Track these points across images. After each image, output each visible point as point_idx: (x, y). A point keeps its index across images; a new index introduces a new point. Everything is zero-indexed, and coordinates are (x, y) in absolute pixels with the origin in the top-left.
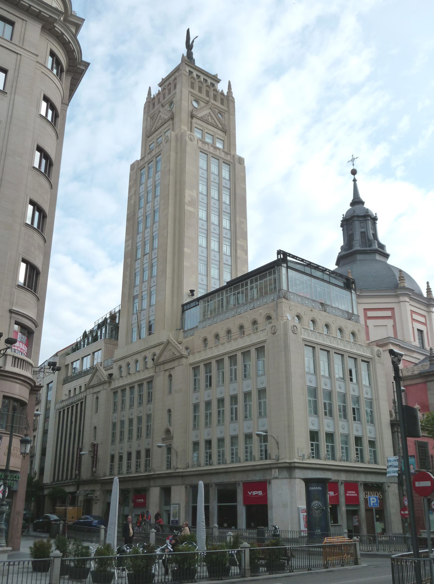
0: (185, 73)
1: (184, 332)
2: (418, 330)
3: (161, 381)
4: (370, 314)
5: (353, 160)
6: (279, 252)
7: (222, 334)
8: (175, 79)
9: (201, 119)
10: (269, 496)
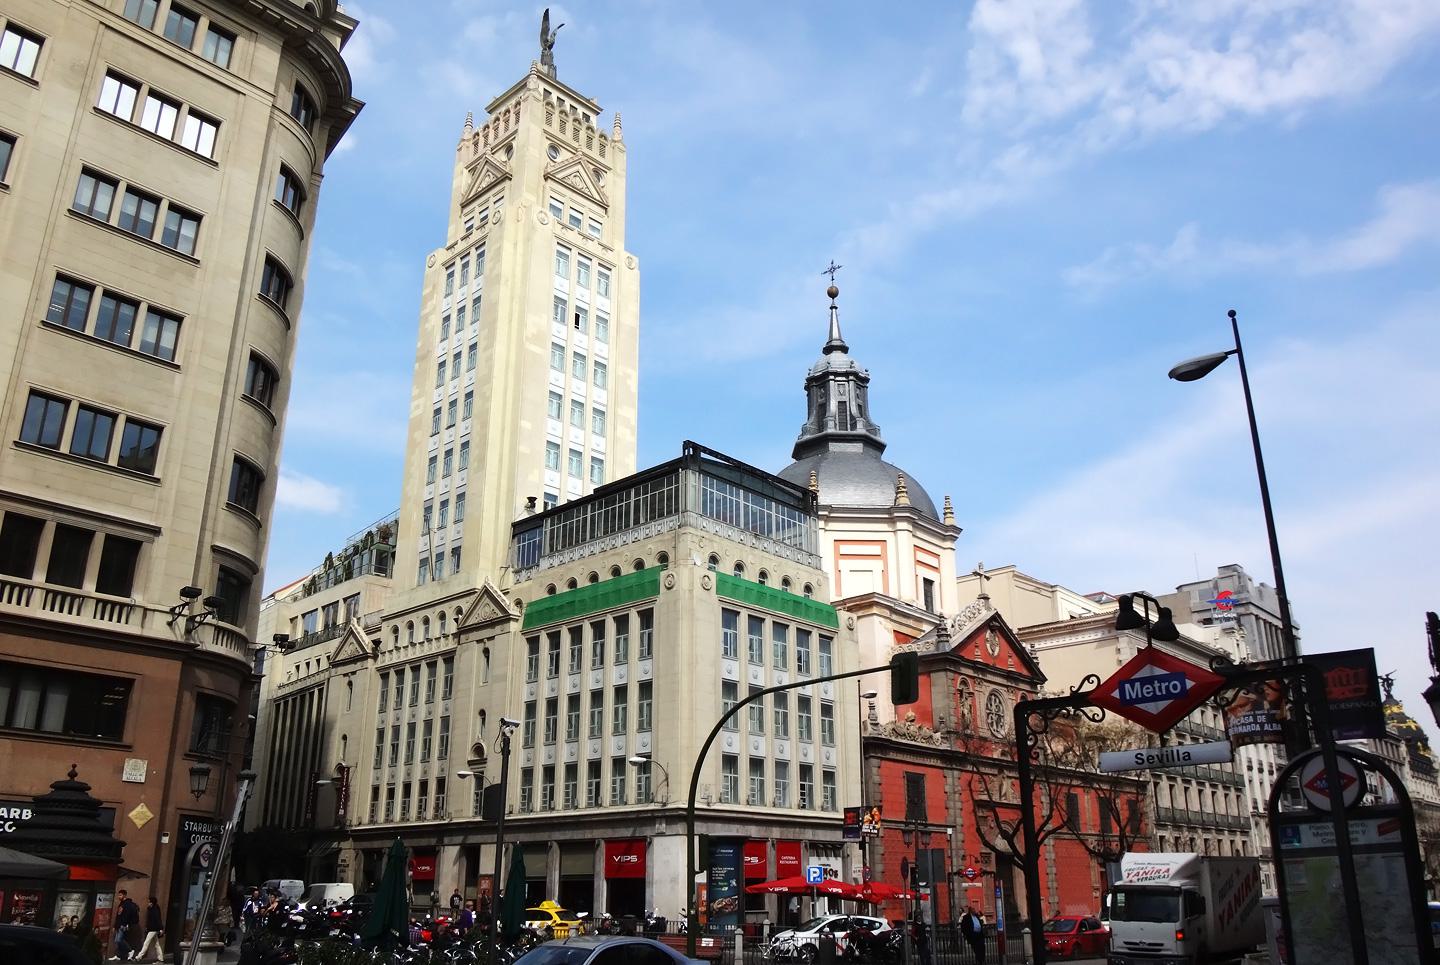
0: (537, 96)
2: (925, 579)
3: (470, 657)
4: (845, 549)
5: (832, 270)
6: (687, 444)
8: (518, 103)
9: (561, 183)
10: (648, 863)
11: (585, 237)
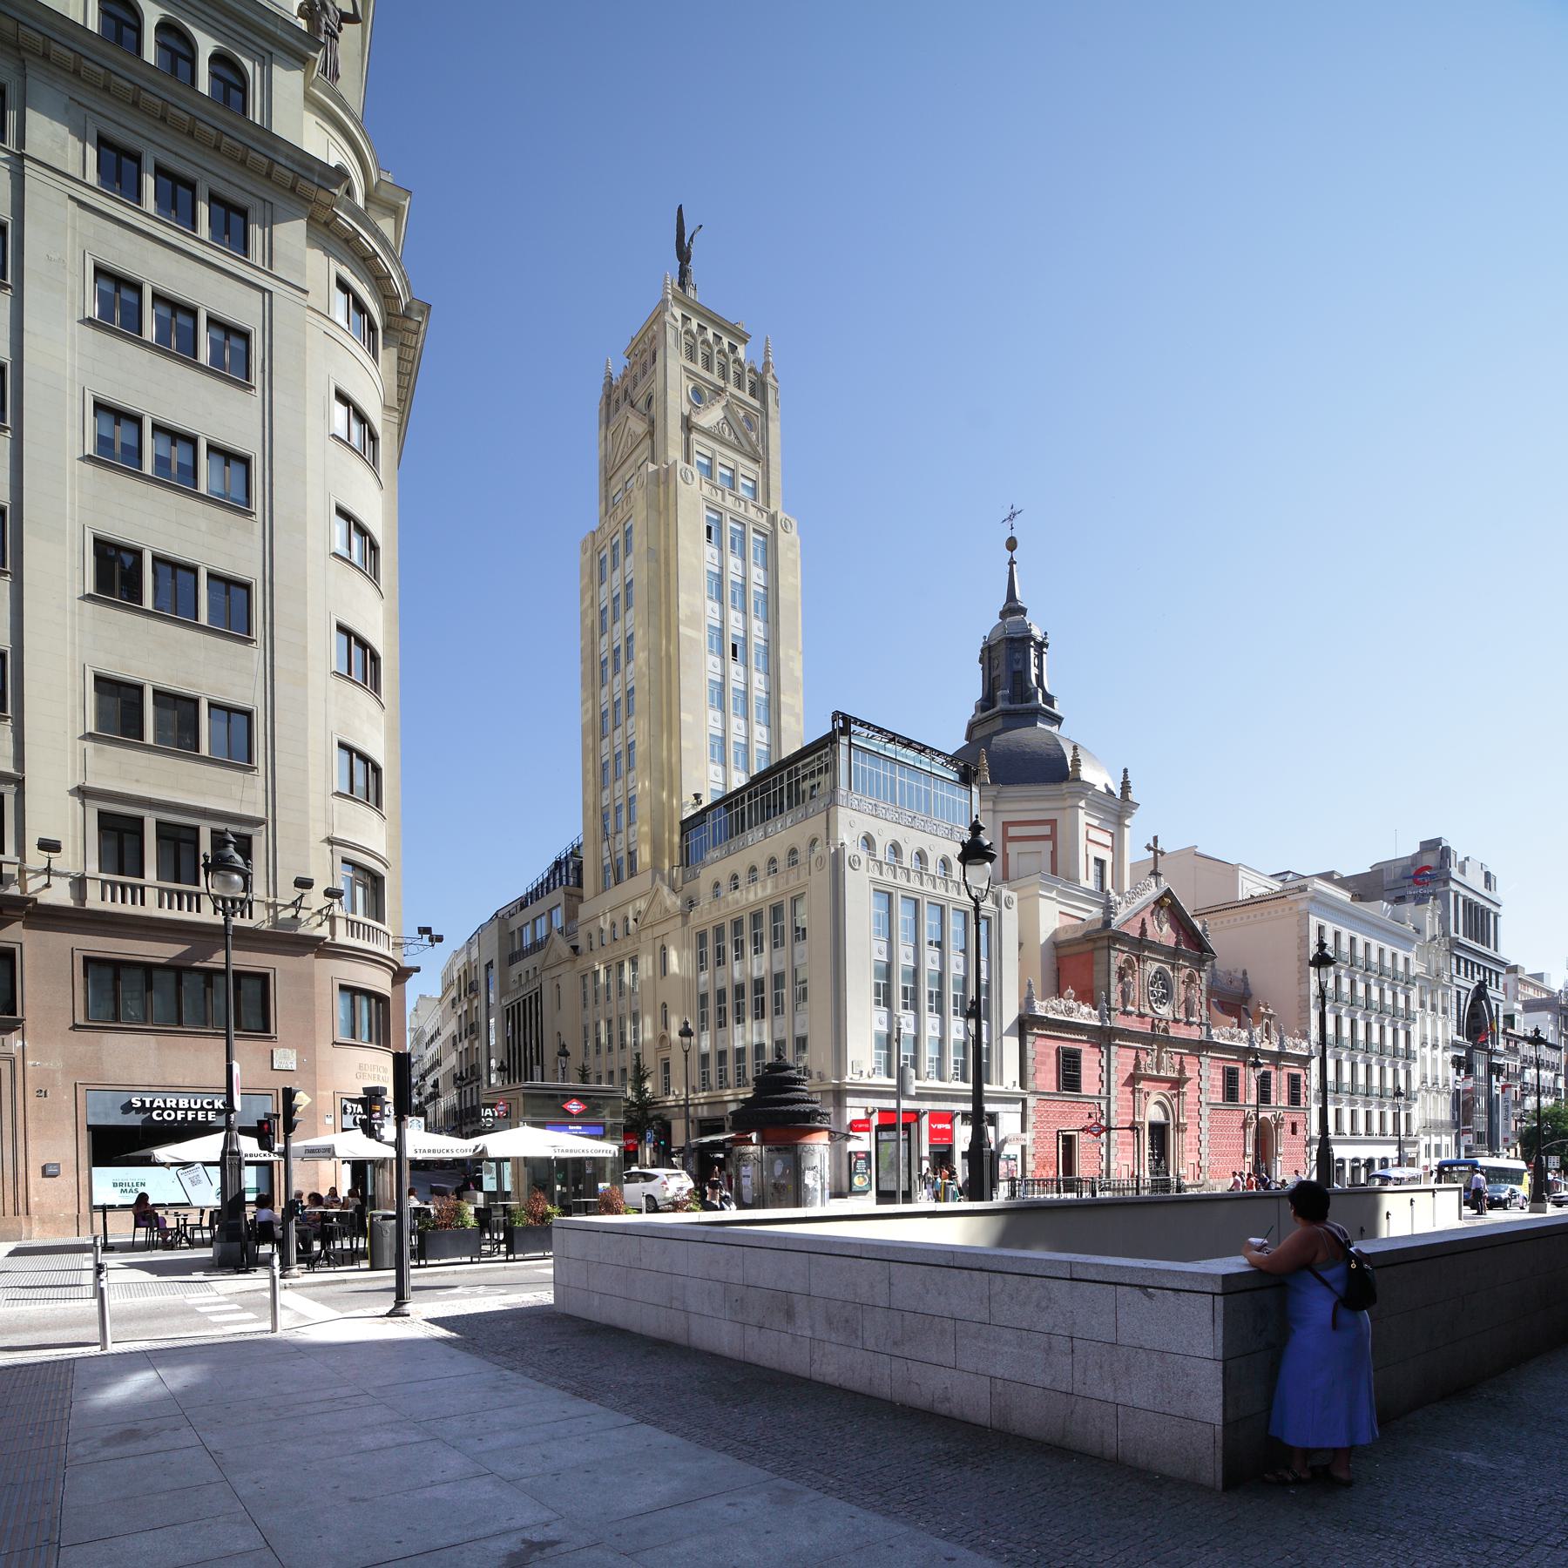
6: (836, 715)
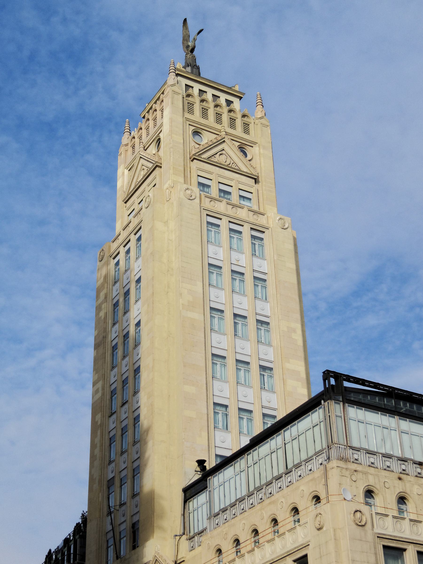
1: (191, 538)
6: (327, 375)
7: (245, 536)
11: (234, 206)
